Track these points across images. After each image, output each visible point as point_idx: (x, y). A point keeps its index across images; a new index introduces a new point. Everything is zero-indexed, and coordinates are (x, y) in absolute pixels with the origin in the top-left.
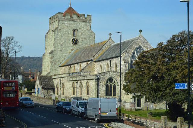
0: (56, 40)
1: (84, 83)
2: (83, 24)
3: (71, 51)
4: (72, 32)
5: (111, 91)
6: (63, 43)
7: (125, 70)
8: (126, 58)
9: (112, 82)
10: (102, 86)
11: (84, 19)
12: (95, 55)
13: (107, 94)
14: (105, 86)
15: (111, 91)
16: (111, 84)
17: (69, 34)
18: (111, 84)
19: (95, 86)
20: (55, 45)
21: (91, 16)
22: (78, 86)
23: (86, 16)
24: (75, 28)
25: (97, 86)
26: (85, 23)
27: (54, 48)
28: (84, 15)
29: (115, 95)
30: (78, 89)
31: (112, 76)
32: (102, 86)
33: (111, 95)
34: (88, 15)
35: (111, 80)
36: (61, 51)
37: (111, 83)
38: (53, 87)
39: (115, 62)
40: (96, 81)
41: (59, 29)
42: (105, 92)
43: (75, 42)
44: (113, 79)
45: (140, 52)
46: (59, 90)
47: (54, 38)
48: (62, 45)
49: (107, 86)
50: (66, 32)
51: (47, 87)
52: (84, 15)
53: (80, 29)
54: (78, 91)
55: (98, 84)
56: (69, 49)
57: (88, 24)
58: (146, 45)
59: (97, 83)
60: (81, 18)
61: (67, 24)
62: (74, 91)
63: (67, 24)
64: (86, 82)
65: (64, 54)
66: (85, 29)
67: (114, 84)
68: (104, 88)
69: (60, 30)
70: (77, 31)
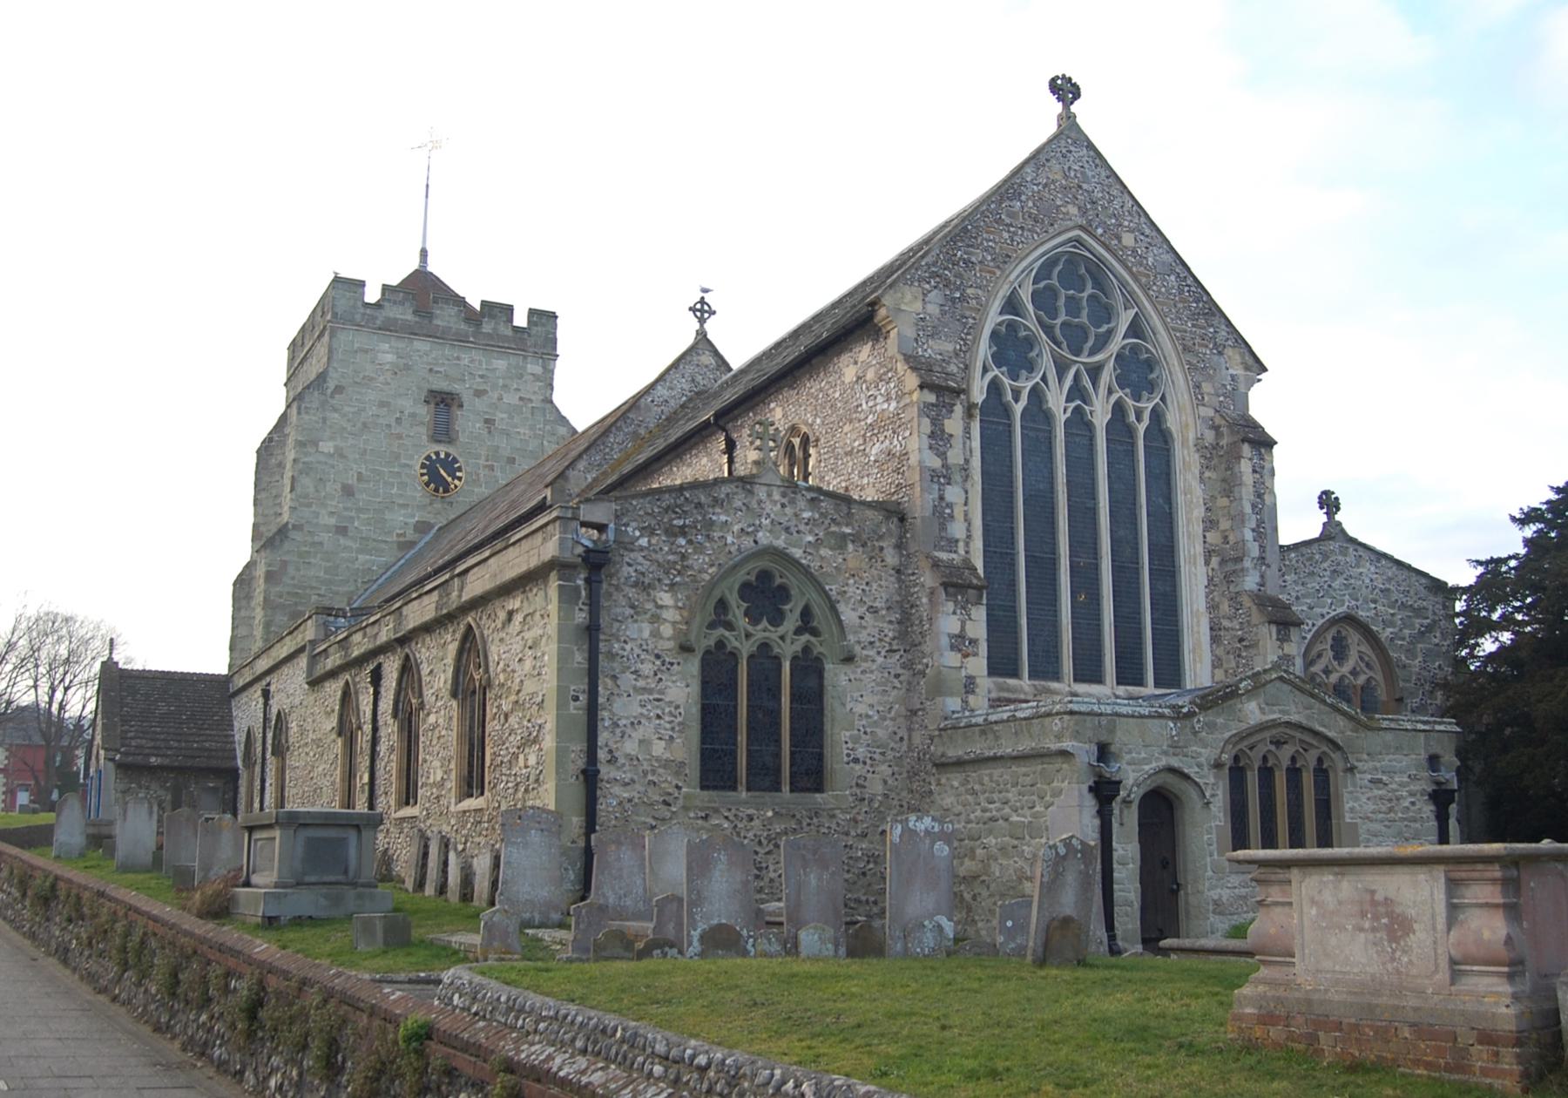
0: (306, 454)
1: (437, 662)
2: (500, 364)
3: (411, 535)
4: (424, 412)
5: (764, 725)
6: (360, 477)
7: (934, 475)
8: (937, 348)
9: (777, 619)
10: (647, 669)
11: (509, 332)
12: (572, 465)
13: (716, 771)
14: (694, 666)
15: (764, 725)
16: (765, 646)
17: (398, 420)
18: (765, 646)
19: (563, 658)
20: (299, 490)
21: (553, 316)
22: (386, 704)
23: (520, 320)
24: (442, 385)
25: (580, 658)
26: (513, 360)
27: (293, 509)
28: (509, 310)
29: (819, 788)
30: (382, 748)
31: (780, 543)
32: (647, 669)
33: (764, 778)
34: (532, 313)
35: (766, 591)
36: (342, 531)
37: (763, 631)
38: (228, 764)
39: (794, 430)
40: (568, 597)
41: (331, 385)
42: (686, 748)
43: (438, 475)
44: (792, 581)
45: (1068, 298)
46: (257, 783)
47: (300, 444)
48: (348, 491)
49: (717, 673)
50: (382, 404)
51: (166, 762)
52: (509, 310)
53: (479, 393)
54: (380, 765)
55: (592, 631)
56: (402, 520)
57: (534, 368)
58: (1128, 240)
59: (581, 617)
60: (487, 327)
61: (390, 358)
62: (350, 775)
63: (390, 358)
64: (453, 648)
65: (360, 551)
66: (511, 399)
67: (807, 649)
68: (682, 690)
69: (339, 389)
70: (461, 406)
